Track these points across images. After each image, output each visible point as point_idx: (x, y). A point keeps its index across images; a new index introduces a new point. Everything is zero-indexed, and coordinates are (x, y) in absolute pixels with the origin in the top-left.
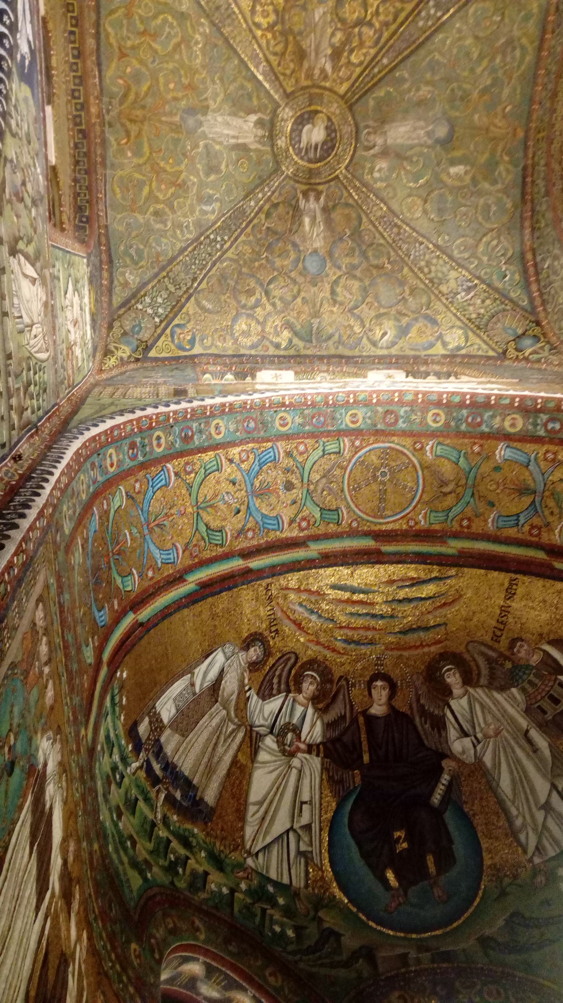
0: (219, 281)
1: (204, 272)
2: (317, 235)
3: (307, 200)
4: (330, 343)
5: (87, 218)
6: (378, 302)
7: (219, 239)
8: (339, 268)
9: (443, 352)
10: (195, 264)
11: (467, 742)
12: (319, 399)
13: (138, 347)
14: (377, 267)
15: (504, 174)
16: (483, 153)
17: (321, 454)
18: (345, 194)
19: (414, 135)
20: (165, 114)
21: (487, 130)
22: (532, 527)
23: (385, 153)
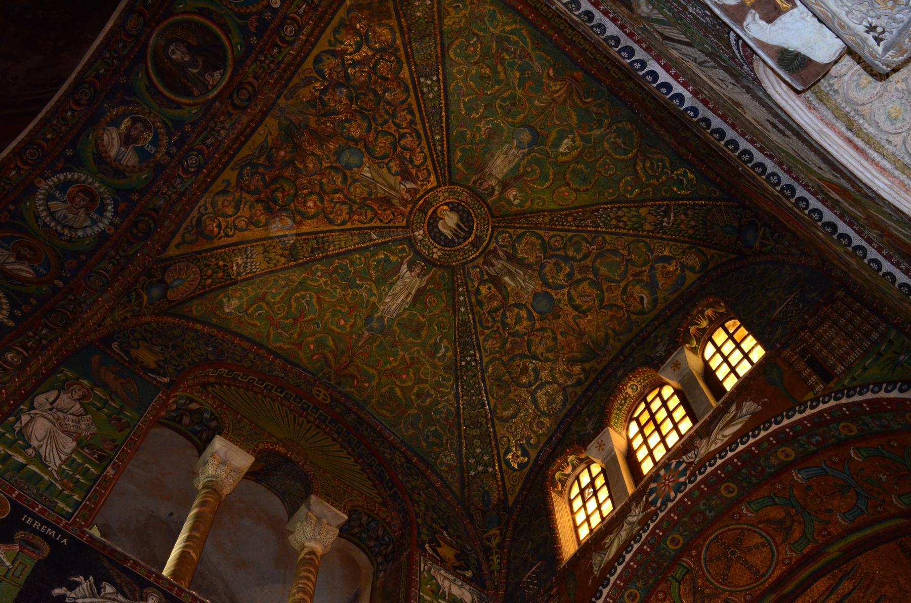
0: (498, 385)
1: (483, 392)
2: (524, 281)
3: (493, 265)
4: (611, 341)
6: (613, 282)
7: (469, 359)
8: (562, 287)
9: (696, 276)
10: (473, 395)
12: (639, 557)
13: (498, 514)
14: (585, 257)
16: (569, 116)
17: (677, 584)
19: (511, 158)
21: (554, 100)
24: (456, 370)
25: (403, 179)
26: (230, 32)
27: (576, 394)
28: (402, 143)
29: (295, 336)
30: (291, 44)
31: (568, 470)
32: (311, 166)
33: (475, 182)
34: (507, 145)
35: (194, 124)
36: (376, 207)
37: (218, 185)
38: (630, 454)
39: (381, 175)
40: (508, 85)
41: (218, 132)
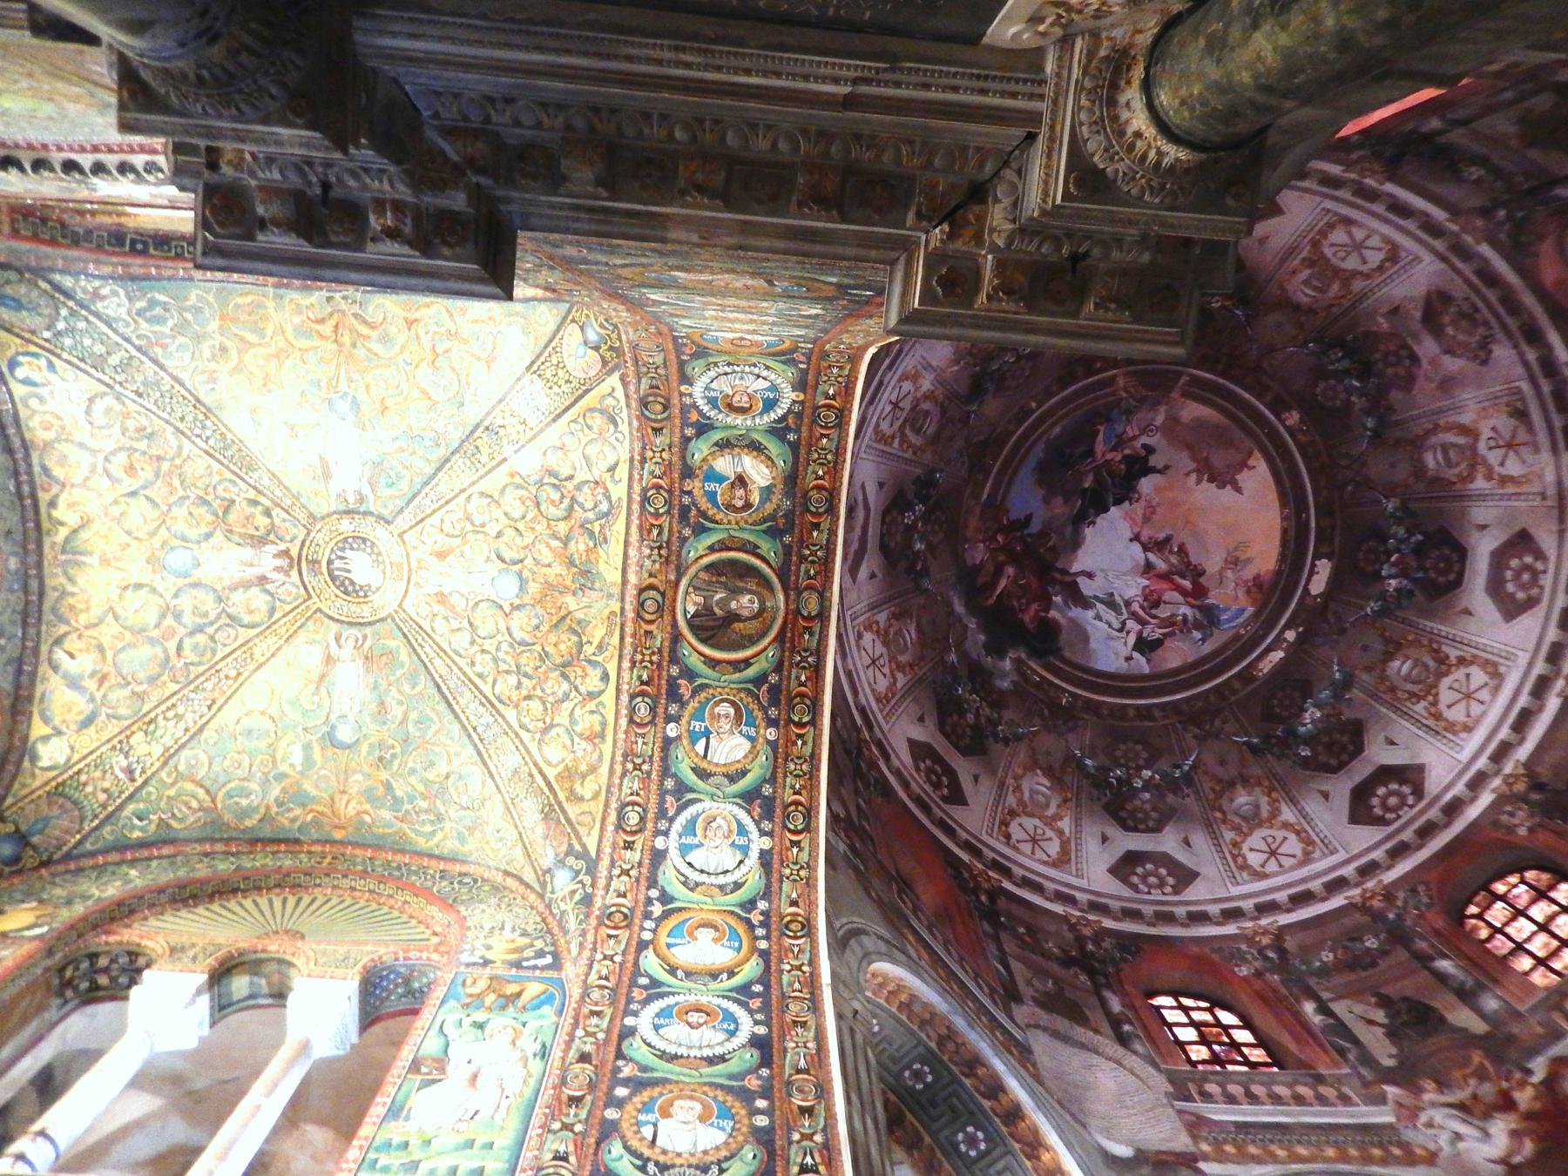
0: (144, 429)
1: (154, 409)
3: (275, 556)
4: (62, 580)
7: (208, 433)
8: (176, 596)
14: (179, 648)
15: (291, 815)
16: (317, 787)
18: (288, 608)
20: (347, 372)
21: (344, 792)
27: (44, 490)
29: (421, 332)
30: (632, 697)
33: (365, 637)
35: (684, 540)
37: (623, 472)
41: (652, 549)
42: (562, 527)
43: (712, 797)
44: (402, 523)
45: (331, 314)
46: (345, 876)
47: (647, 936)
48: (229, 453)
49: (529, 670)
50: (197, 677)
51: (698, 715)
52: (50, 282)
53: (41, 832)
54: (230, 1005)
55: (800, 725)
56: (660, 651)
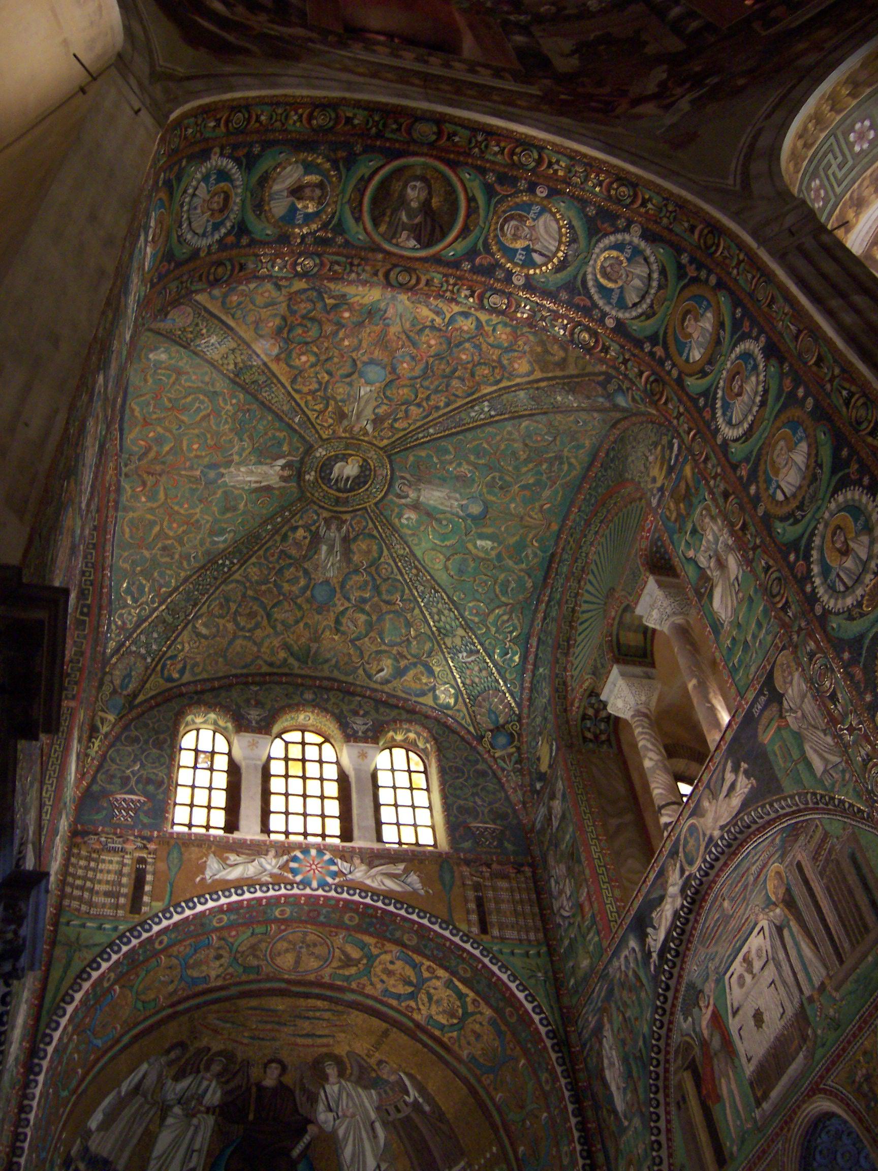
0: (221, 604)
2: (333, 565)
3: (328, 528)
4: (326, 666)
5: (88, 606)
6: (381, 639)
7: (227, 562)
8: (348, 600)
11: (330, 1116)
12: (253, 902)
14: (388, 603)
16: (514, 535)
18: (371, 525)
20: (185, 469)
21: (522, 518)
22: (408, 1006)
23: (416, 506)
24: (211, 561)
25: (374, 422)
26: (464, 238)
27: (260, 667)
28: (412, 408)
29: (154, 416)
30: (482, 307)
31: (199, 720)
32: (346, 343)
33: (403, 478)
34: (458, 496)
35: (347, 243)
36: (330, 409)
38: (266, 775)
39: (367, 402)
40: (518, 477)
41: (351, 271)
42: (329, 329)
43: (585, 263)
44: (311, 438)
45: (139, 476)
46: (585, 536)
47: (675, 373)
48: (245, 551)
49: (448, 370)
50: (413, 595)
51: (510, 253)
52: (112, 656)
53: (497, 717)
54: (645, 649)
55: (539, 162)
56: (445, 275)
